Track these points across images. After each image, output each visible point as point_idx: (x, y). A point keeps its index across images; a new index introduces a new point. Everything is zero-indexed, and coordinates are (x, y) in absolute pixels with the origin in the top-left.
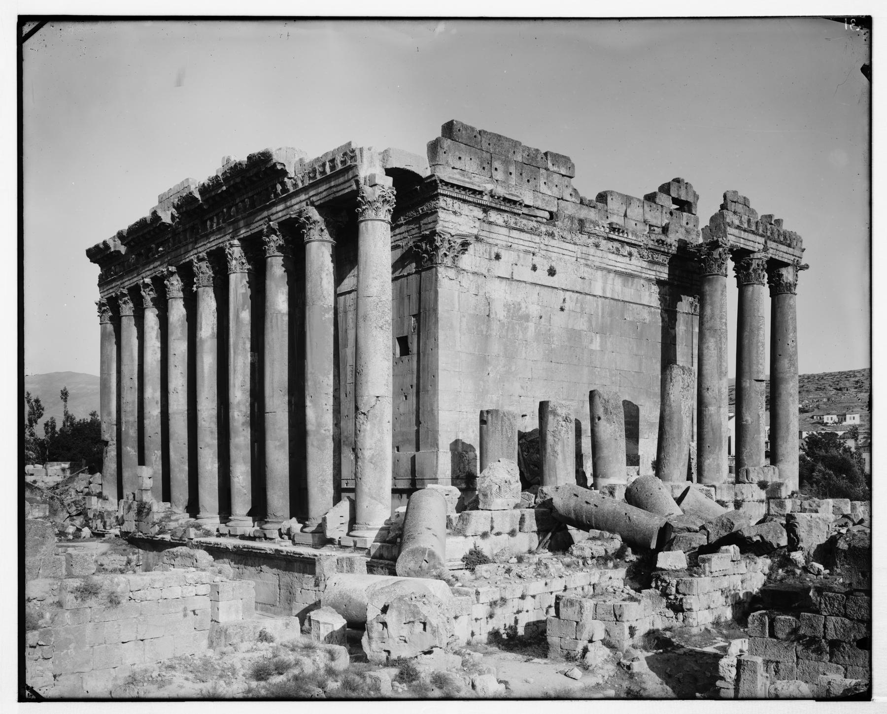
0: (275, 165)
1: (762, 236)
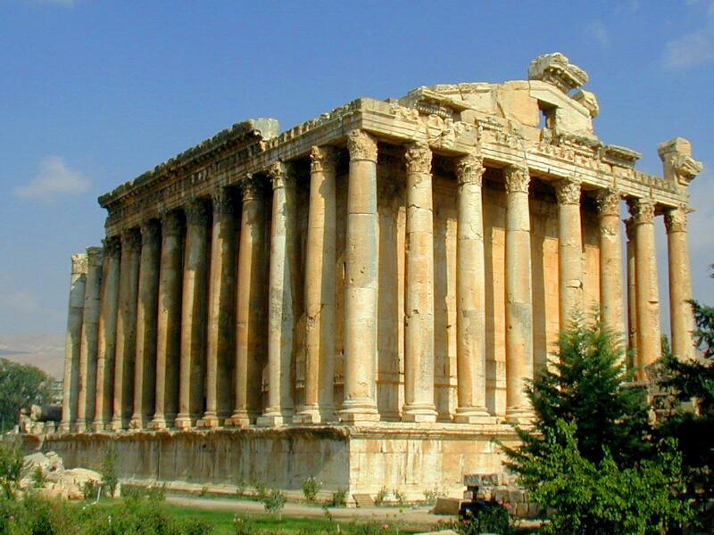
0: (253, 132)
1: (647, 186)
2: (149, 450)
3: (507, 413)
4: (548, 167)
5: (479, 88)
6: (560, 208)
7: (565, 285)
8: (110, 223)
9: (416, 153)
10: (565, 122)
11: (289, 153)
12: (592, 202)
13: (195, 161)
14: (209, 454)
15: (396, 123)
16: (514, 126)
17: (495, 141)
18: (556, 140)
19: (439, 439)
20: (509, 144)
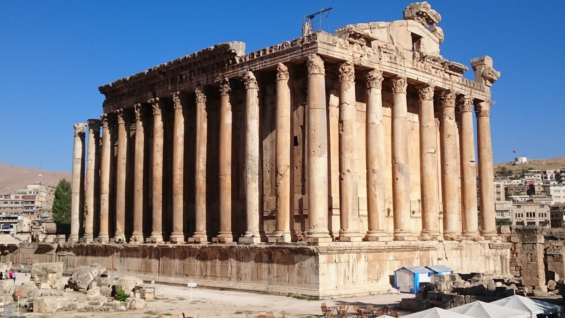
0: (231, 50)
1: (469, 87)
3: (394, 233)
4: (417, 76)
5: (380, 25)
6: (421, 102)
7: (425, 151)
8: (105, 104)
9: (346, 68)
10: (425, 47)
12: (440, 96)
13: (182, 67)
15: (337, 49)
16: (400, 50)
17: (389, 60)
18: (423, 58)
19: (367, 252)
20: (397, 62)
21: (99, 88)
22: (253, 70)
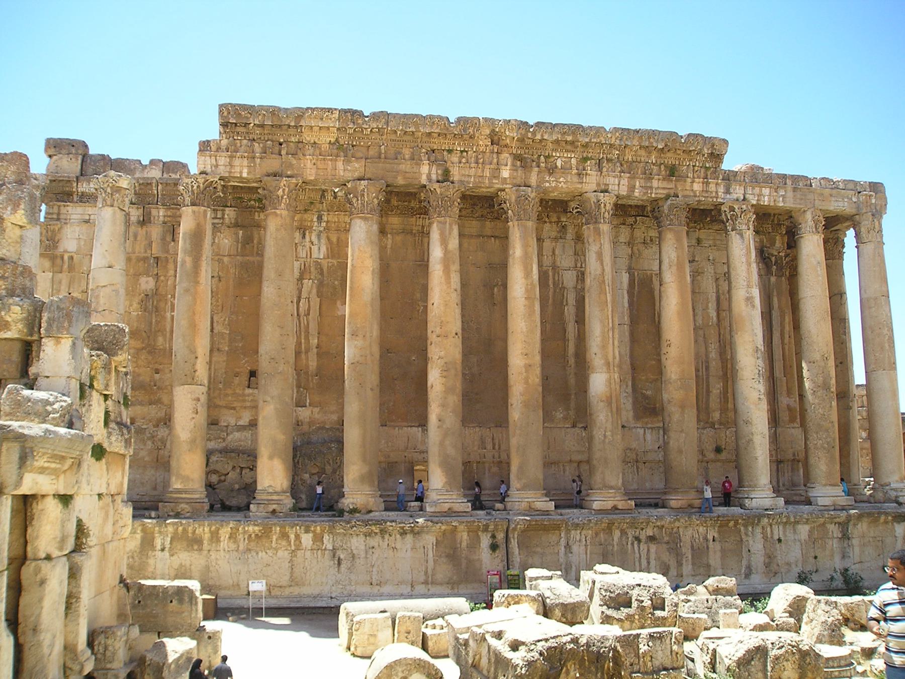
2: (474, 543)
11: (766, 198)
14: (665, 546)
21: (221, 106)
22: (754, 202)
